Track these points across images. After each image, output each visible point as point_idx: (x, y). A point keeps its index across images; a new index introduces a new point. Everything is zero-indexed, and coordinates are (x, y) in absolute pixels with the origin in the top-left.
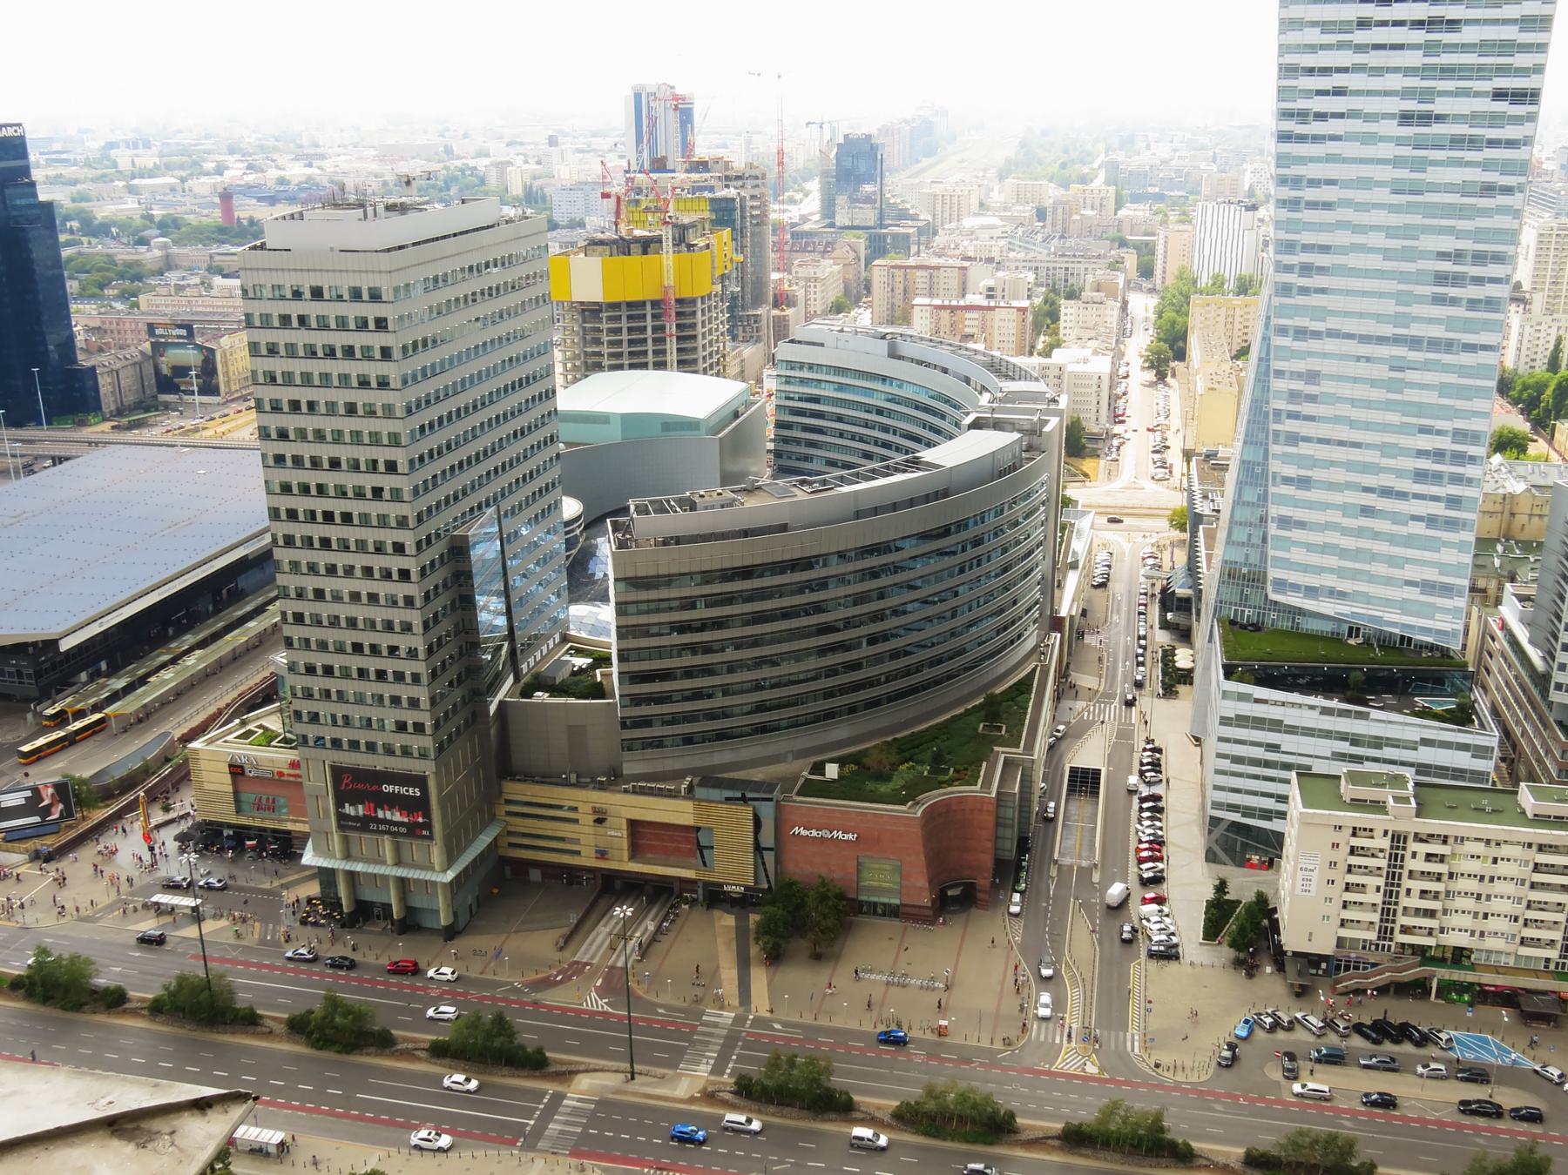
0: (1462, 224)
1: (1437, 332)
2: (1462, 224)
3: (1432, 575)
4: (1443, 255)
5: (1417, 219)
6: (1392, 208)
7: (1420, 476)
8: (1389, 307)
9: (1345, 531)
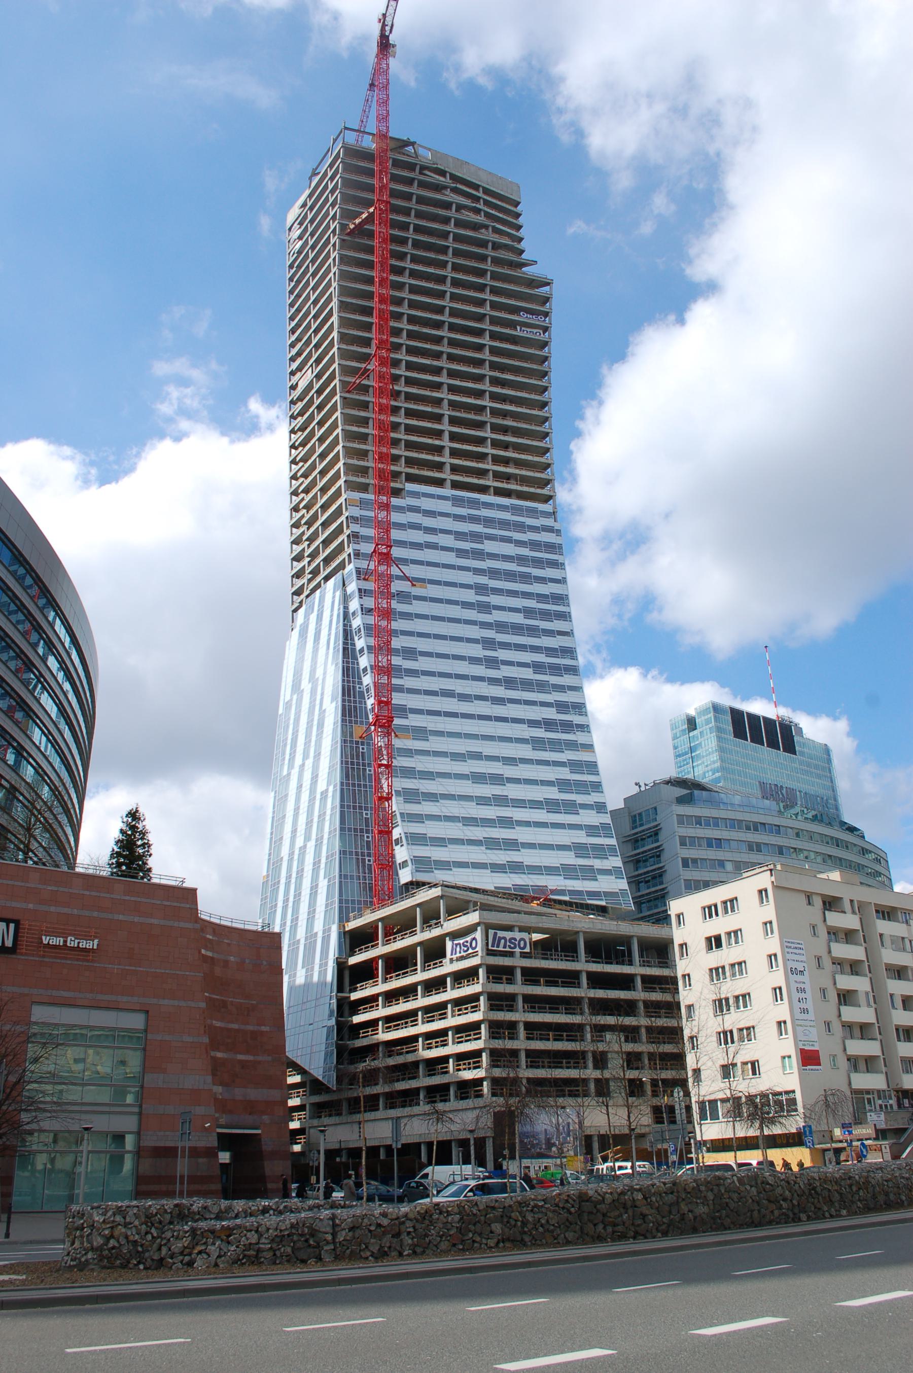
0: (517, 536)
1: (518, 619)
2: (517, 536)
3: (581, 837)
5: (478, 528)
6: (458, 518)
7: (538, 744)
8: (470, 596)
9: (483, 801)
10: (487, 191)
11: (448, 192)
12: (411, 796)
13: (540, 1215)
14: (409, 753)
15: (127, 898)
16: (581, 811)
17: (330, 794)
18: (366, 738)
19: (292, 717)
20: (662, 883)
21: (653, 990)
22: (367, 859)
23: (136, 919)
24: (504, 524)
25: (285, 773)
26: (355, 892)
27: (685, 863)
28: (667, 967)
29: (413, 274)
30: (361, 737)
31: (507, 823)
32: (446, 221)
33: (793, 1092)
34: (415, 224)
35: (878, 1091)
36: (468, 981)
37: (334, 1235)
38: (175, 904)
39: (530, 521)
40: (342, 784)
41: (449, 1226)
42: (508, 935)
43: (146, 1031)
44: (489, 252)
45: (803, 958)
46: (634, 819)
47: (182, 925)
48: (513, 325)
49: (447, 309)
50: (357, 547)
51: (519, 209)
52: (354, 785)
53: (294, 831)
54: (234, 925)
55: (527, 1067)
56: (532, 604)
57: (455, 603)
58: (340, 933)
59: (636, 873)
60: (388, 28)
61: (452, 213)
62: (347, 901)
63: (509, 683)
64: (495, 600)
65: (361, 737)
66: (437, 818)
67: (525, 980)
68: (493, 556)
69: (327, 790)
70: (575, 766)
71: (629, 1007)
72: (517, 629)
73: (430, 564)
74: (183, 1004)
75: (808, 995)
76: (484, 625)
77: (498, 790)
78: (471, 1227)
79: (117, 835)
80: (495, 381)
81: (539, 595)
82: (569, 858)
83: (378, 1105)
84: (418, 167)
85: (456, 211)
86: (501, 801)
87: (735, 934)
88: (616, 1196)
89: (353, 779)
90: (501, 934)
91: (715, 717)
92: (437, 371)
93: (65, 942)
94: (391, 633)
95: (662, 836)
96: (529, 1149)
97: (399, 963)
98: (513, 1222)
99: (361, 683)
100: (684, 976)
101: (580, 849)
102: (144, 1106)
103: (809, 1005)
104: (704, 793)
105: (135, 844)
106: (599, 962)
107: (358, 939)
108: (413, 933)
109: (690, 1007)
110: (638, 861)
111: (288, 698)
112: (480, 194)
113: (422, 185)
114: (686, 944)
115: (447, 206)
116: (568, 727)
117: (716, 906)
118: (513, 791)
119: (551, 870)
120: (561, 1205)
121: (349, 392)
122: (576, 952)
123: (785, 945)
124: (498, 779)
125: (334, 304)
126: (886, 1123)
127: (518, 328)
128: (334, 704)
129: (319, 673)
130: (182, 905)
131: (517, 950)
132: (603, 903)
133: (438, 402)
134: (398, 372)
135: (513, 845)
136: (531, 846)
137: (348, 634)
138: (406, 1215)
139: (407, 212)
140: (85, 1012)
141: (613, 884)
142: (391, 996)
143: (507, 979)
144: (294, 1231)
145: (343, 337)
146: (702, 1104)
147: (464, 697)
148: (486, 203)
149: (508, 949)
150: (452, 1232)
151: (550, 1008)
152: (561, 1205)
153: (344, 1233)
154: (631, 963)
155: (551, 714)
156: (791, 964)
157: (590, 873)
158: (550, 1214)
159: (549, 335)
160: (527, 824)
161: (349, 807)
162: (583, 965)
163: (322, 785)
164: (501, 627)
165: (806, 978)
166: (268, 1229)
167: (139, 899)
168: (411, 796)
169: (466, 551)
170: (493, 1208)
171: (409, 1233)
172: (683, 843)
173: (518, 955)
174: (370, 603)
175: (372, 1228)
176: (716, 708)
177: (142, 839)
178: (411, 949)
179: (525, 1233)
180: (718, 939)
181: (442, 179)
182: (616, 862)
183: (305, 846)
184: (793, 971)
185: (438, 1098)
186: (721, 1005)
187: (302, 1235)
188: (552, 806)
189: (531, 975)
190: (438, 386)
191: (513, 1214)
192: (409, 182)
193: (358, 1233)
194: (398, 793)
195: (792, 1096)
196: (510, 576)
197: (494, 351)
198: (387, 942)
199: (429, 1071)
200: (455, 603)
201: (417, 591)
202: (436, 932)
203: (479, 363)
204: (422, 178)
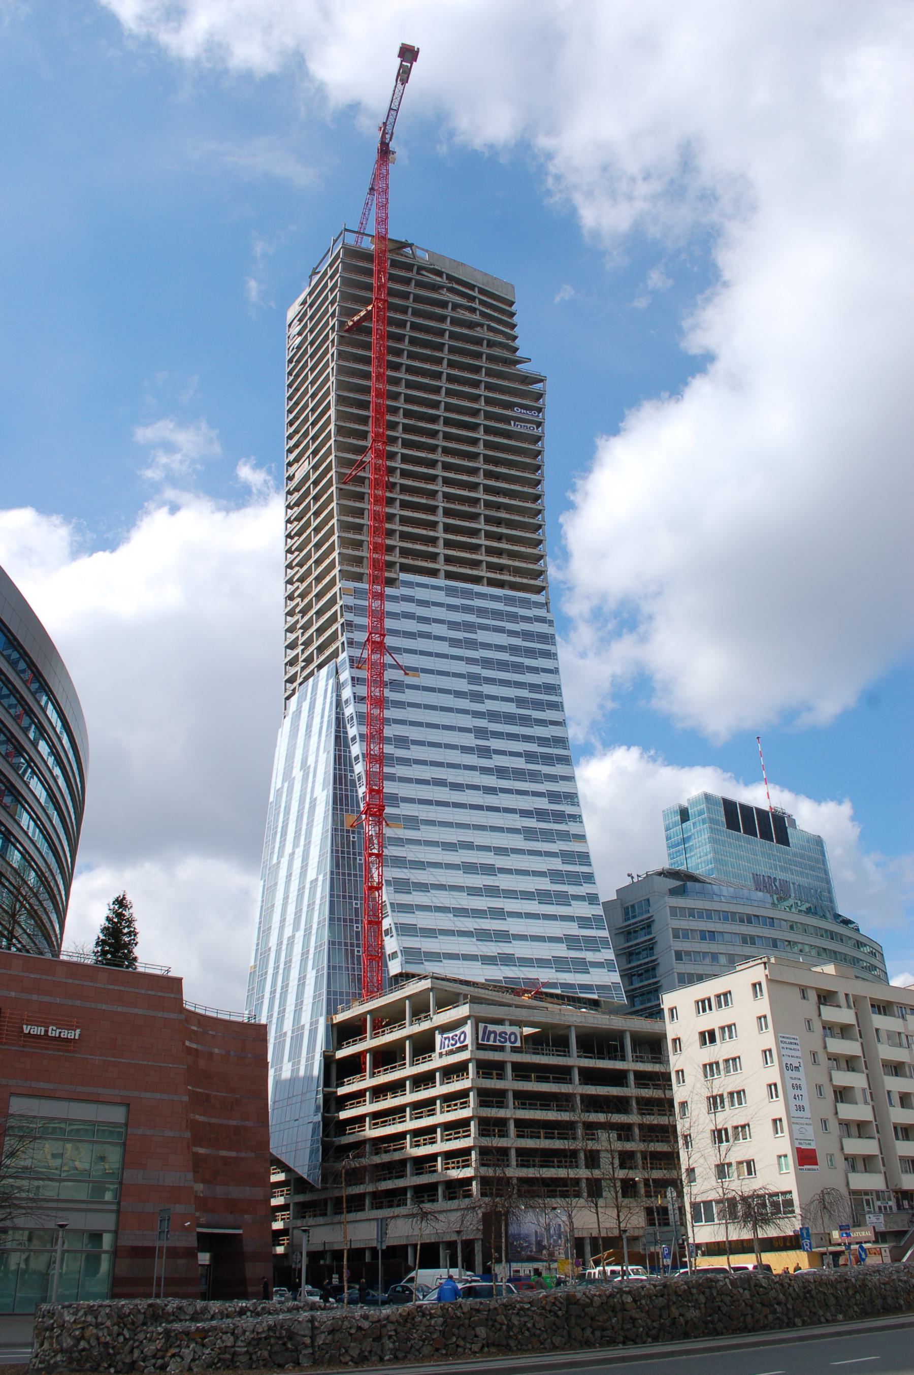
1: (511, 708)
3: (573, 929)
4: (500, 648)
5: (471, 618)
6: (451, 607)
7: (529, 834)
9: (474, 891)
10: (482, 291)
11: (444, 291)
12: (401, 886)
13: (526, 1319)
14: (400, 842)
15: (111, 987)
16: (573, 902)
17: (320, 883)
18: (357, 827)
19: (283, 805)
20: (655, 976)
21: (646, 1086)
22: (356, 949)
23: (120, 1009)
24: (497, 615)
25: (275, 861)
26: (343, 984)
27: (679, 956)
28: (660, 1063)
29: (410, 370)
30: (352, 826)
31: (498, 913)
32: (442, 319)
33: (790, 1192)
34: (412, 322)
35: (877, 1192)
36: (458, 1076)
37: (313, 1338)
38: (160, 994)
39: (523, 612)
40: (332, 873)
41: (432, 1329)
42: (498, 1029)
43: (126, 1125)
44: (484, 349)
45: (798, 1054)
46: (626, 911)
47: (166, 1015)
48: (507, 420)
49: (443, 404)
50: (351, 635)
51: (513, 308)
52: (344, 874)
53: (283, 921)
54: (220, 1016)
55: (517, 1166)
56: (524, 693)
57: (448, 692)
58: (327, 1026)
59: (630, 966)
60: (388, 136)
61: (448, 312)
62: (335, 993)
63: (501, 772)
64: (487, 689)
65: (352, 826)
66: (427, 908)
67: (516, 1076)
68: (486, 646)
69: (316, 880)
70: (567, 857)
71: (621, 1104)
72: (510, 718)
73: (423, 653)
74: (165, 1097)
75: (804, 1092)
76: (477, 714)
77: (489, 881)
78: (455, 1331)
79: (103, 922)
80: (489, 475)
81: (531, 685)
82: (561, 950)
83: (364, 1205)
84: (416, 267)
85: (453, 309)
86: (493, 891)
87: (729, 1029)
88: (604, 1298)
89: (343, 868)
90: (491, 1027)
91: (708, 808)
92: (432, 464)
93: (46, 1031)
94: (384, 721)
95: (655, 928)
96: (518, 1252)
97: (387, 1057)
98: (498, 1326)
99: (352, 771)
100: (677, 1072)
101: (572, 941)
102: (122, 1203)
103: (805, 1102)
104: (697, 884)
105: (121, 932)
106: (591, 1058)
107: (345, 1032)
108: (402, 1026)
109: (683, 1105)
110: (631, 954)
111: (279, 786)
112: (476, 294)
113: (420, 284)
114: (679, 1039)
115: (444, 304)
116: (560, 817)
117: (709, 1000)
118: (504, 882)
119: (542, 963)
120: (548, 1308)
121: (345, 483)
122: (568, 1047)
123: (780, 1040)
124: (489, 870)
125: (332, 398)
126: (886, 1226)
127: (512, 423)
128: (326, 791)
129: (311, 761)
130: (167, 995)
131: (508, 1044)
132: (595, 997)
133: (433, 494)
134: (393, 464)
135: (504, 936)
136: (523, 938)
137: (340, 722)
138: (387, 1318)
139: (404, 310)
140: (63, 1105)
141: (604, 976)
142: (379, 1092)
143: (497, 1074)
144: (271, 1334)
145: (340, 430)
146: (695, 1206)
147: (456, 787)
148: (482, 302)
149: (498, 1044)
150: (435, 1336)
151: (541, 1105)
152: (548, 1308)
153: (323, 1336)
154: (623, 1058)
155: (543, 803)
156: (786, 1060)
157: (582, 966)
158: (537, 1318)
159: (543, 430)
160: (518, 915)
161: (338, 896)
162: (575, 1060)
163: (311, 874)
164: (493, 716)
165: (801, 1074)
166: (245, 1331)
167: (123, 988)
168: (401, 886)
169: (459, 641)
170: (478, 1311)
171: (390, 1337)
172: (676, 936)
173: (508, 1049)
174: (363, 691)
175: (353, 1331)
176: (707, 797)
177: (129, 927)
178: (400, 1043)
179: (510, 1337)
180: (712, 1034)
181: (438, 279)
182: (609, 954)
183: (293, 936)
184: (789, 1067)
185: (426, 1198)
186: (715, 1102)
187: (279, 1338)
188: (543, 896)
189: (522, 1071)
190: (433, 479)
191: (498, 1318)
192: (407, 281)
193: (338, 1336)
194: (388, 883)
195: (788, 1197)
196: (503, 665)
197: (488, 445)
198: (375, 1035)
199: (417, 1169)
200: (448, 692)
201: (410, 680)
202: (425, 1025)
203: (474, 456)
204: (419, 277)
